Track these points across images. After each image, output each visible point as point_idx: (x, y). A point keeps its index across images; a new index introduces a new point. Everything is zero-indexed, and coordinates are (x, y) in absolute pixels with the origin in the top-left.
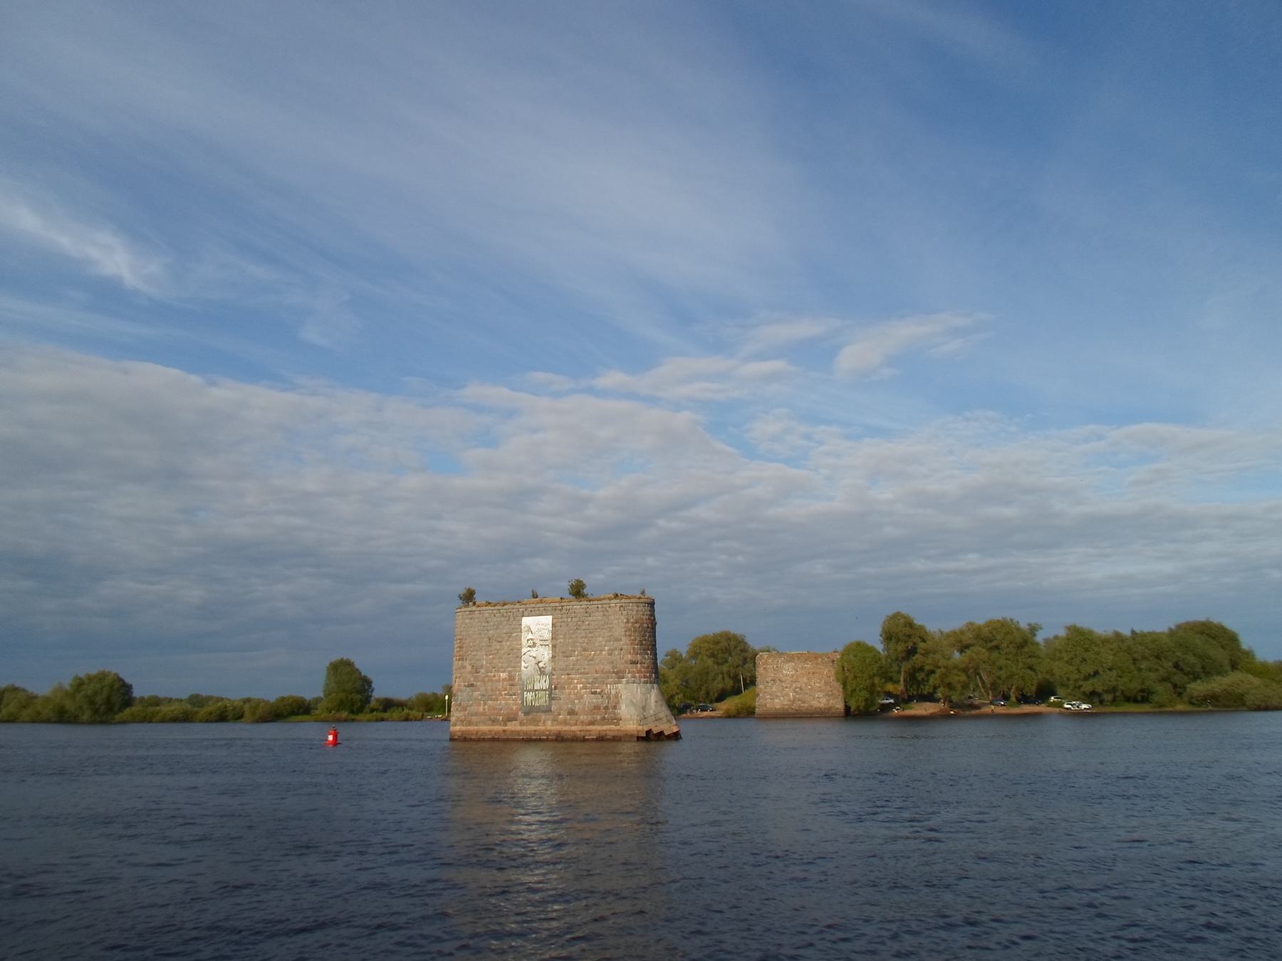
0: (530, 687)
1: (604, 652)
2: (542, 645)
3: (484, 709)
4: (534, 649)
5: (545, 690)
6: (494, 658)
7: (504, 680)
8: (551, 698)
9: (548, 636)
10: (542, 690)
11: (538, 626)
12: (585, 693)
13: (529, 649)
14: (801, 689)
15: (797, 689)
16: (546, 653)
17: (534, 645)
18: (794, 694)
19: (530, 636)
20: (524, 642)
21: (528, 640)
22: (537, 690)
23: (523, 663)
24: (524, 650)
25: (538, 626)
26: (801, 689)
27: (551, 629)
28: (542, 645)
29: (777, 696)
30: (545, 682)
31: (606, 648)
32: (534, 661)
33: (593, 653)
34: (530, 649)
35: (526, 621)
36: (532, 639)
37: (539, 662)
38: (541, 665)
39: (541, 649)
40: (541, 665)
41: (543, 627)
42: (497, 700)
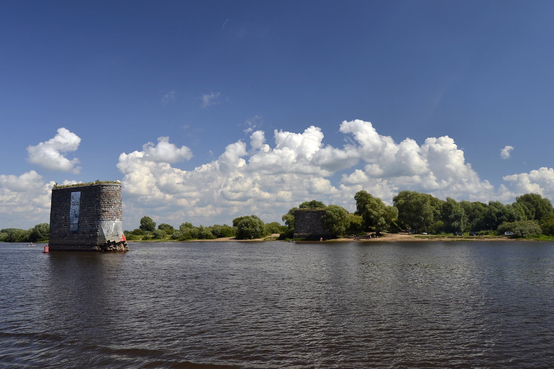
0: (72, 223)
1: (94, 207)
2: (77, 204)
3: (57, 232)
4: (74, 206)
6: (61, 210)
7: (64, 219)
8: (79, 227)
10: (76, 224)
12: (88, 225)
13: (73, 206)
14: (313, 225)
15: (311, 225)
16: (78, 208)
18: (310, 227)
19: (73, 201)
20: (71, 203)
21: (73, 202)
22: (74, 224)
24: (71, 207)
26: (313, 225)
27: (80, 197)
28: (77, 204)
29: (303, 228)
31: (95, 205)
32: (74, 212)
33: (91, 207)
35: (72, 193)
37: (75, 212)
38: (76, 213)
39: (76, 206)
40: (76, 213)
42: (61, 228)
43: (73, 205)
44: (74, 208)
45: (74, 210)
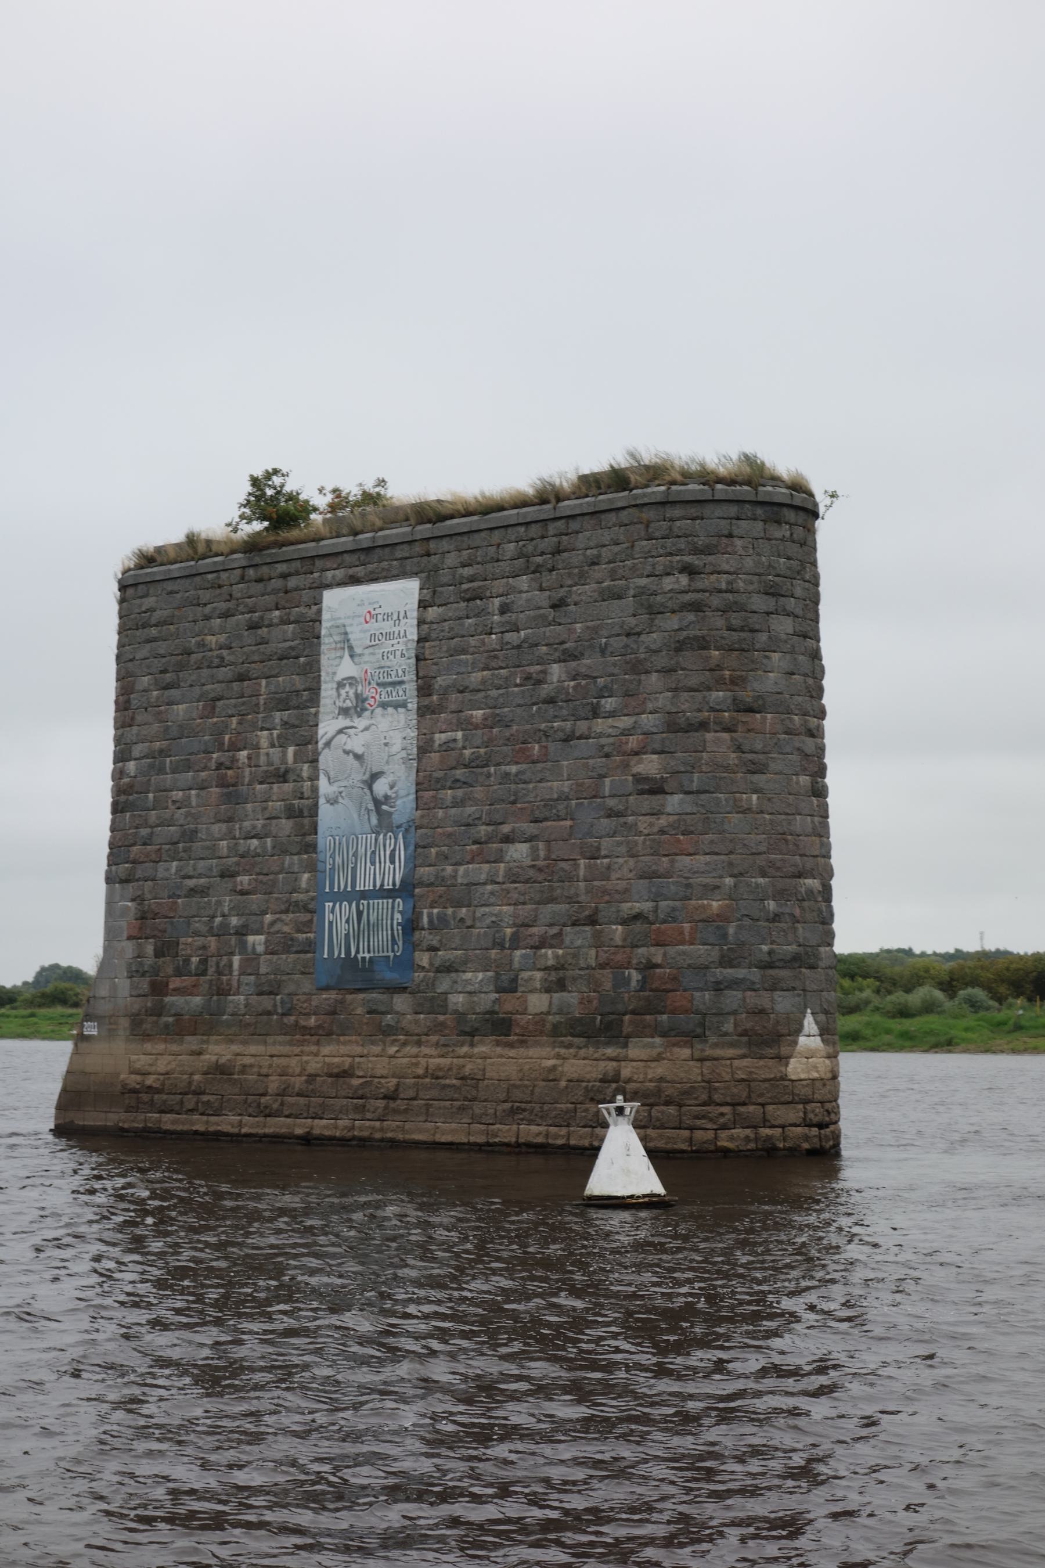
0: (341, 883)
2: (384, 705)
4: (361, 723)
5: (390, 894)
9: (403, 666)
10: (382, 893)
11: (374, 626)
13: (342, 722)
17: (360, 706)
19: (347, 668)
21: (340, 685)
22: (364, 895)
23: (323, 784)
24: (327, 727)
25: (374, 626)
30: (392, 862)
32: (358, 775)
34: (347, 722)
35: (331, 598)
36: (352, 681)
37: (375, 776)
38: (381, 787)
40: (381, 787)
41: (387, 626)
43: (344, 712)
44: (356, 743)
45: (358, 757)
